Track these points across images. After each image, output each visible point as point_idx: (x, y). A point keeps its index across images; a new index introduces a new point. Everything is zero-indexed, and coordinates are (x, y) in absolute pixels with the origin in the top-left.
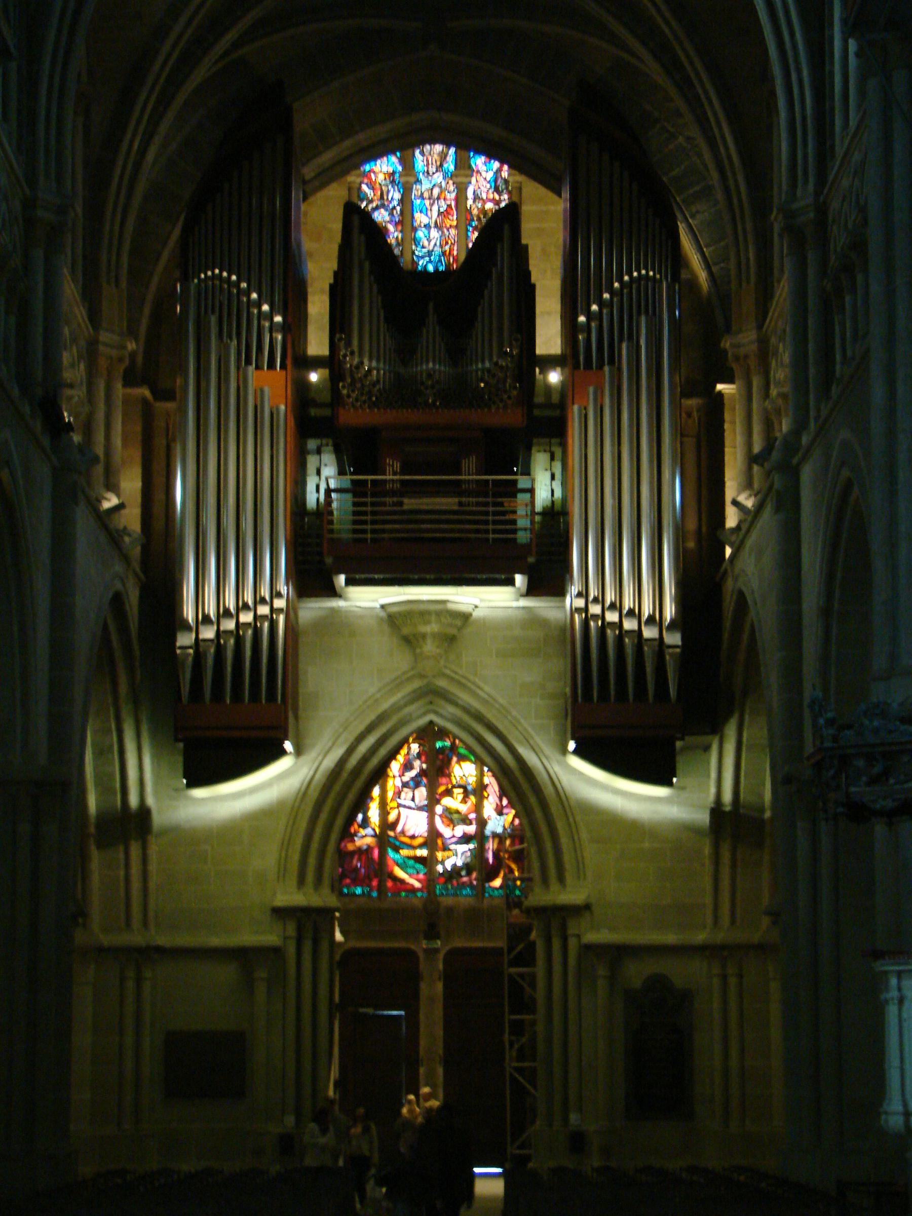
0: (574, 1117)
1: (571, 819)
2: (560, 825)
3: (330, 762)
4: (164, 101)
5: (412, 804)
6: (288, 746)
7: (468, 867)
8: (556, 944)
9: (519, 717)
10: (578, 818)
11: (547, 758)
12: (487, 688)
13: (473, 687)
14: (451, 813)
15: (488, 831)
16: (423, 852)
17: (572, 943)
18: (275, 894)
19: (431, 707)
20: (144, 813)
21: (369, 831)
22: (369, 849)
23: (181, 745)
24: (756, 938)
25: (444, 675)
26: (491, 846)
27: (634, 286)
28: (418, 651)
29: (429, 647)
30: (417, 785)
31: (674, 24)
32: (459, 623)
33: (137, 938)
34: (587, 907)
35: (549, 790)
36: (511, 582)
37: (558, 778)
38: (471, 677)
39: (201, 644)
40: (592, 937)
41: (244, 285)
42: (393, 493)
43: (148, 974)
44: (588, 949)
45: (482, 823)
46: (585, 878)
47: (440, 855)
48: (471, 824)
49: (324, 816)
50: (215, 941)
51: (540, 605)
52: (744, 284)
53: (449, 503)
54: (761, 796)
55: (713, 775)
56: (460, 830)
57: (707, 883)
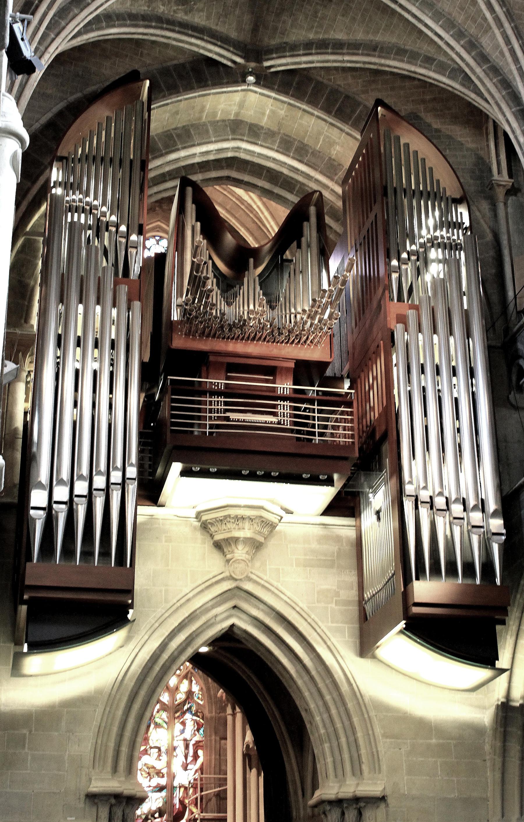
1: (366, 716)
3: (145, 655)
9: (316, 619)
10: (372, 714)
12: (288, 593)
13: (276, 591)
15: (176, 784)
18: (90, 780)
19: (234, 612)
25: (249, 579)
26: (178, 794)
28: (229, 556)
32: (266, 531)
34: (383, 799)
35: (344, 688)
36: (329, 482)
37: (353, 677)
38: (275, 584)
39: (55, 506)
45: (172, 777)
46: (380, 772)
49: (136, 706)
56: (157, 781)
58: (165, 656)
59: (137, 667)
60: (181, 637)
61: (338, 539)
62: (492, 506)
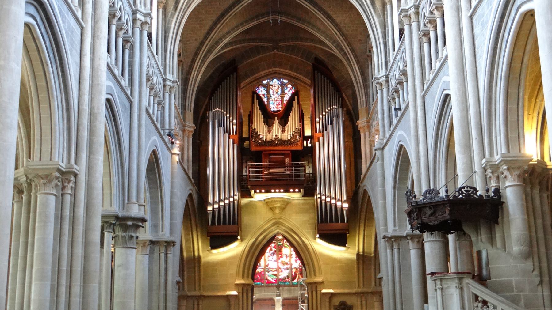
2: (315, 260)
4: (203, 62)
5: (272, 260)
6: (239, 237)
7: (288, 277)
8: (314, 293)
10: (319, 257)
11: (310, 240)
12: (293, 222)
14: (283, 262)
15: (293, 267)
16: (276, 273)
17: (319, 292)
19: (278, 228)
20: (199, 257)
21: (261, 267)
22: (261, 272)
23: (209, 237)
24: (370, 290)
26: (294, 270)
27: (332, 110)
29: (277, 211)
30: (274, 254)
31: (341, 38)
33: (197, 293)
34: (322, 282)
35: (311, 250)
38: (289, 219)
40: (324, 291)
41: (225, 113)
42: (267, 167)
43: (201, 303)
45: (291, 265)
46: (322, 274)
47: (280, 273)
48: (288, 265)
49: (249, 258)
52: (362, 107)
53: (282, 170)
54: (371, 249)
55: (357, 244)
56: (286, 266)
57: (356, 274)
58: (257, 243)
59: (248, 248)
60: (261, 237)
62: (345, 198)
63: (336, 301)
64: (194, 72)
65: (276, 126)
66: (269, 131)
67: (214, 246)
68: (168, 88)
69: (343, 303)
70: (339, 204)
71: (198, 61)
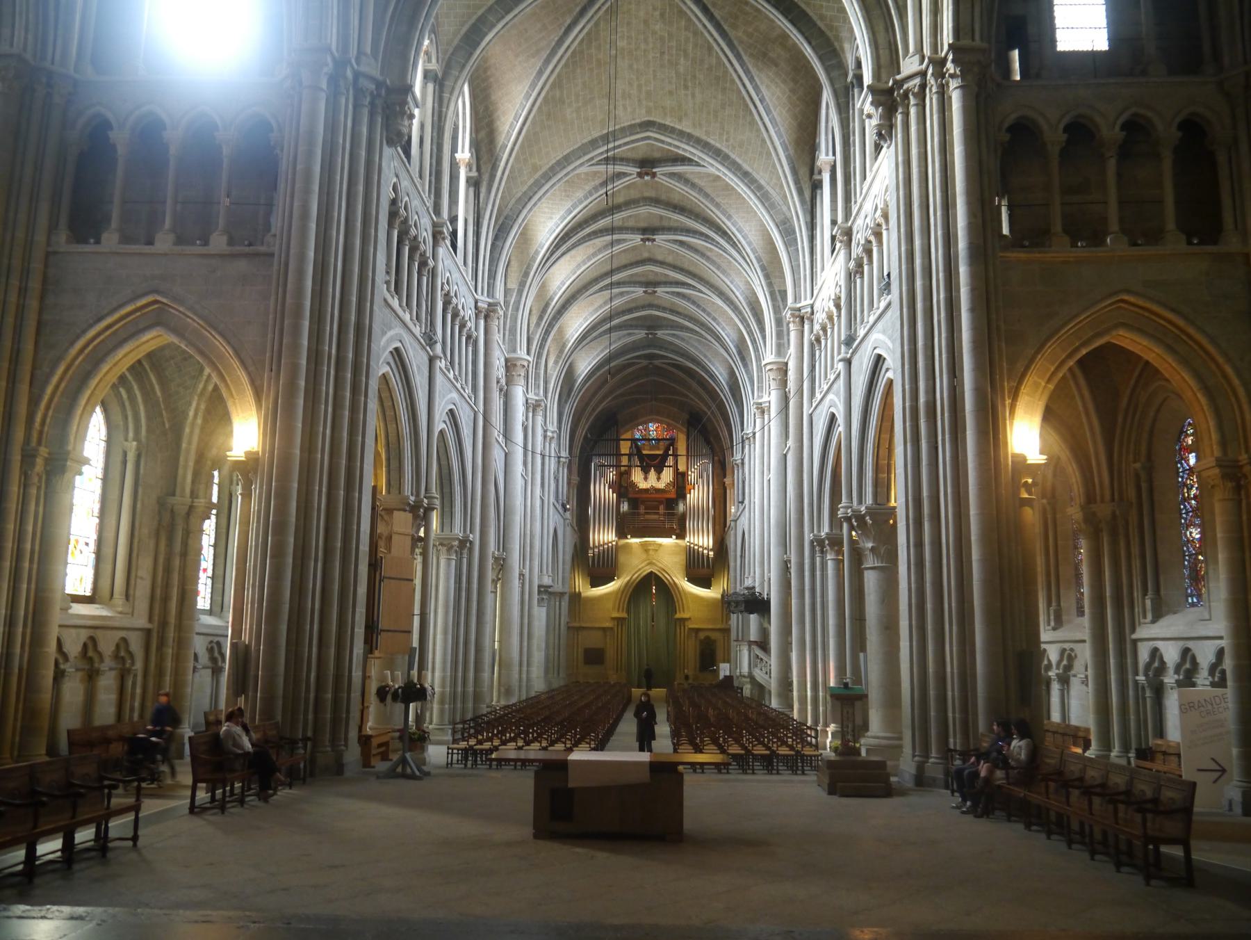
0: (686, 671)
4: (588, 420)
20: (580, 593)
29: (651, 552)
34: (690, 619)
40: (691, 626)
44: (690, 629)
50: (597, 625)
51: (678, 541)
60: (636, 575)
61: (680, 546)
62: (711, 546)
63: (702, 635)
64: (579, 431)
65: (652, 474)
66: (646, 479)
67: (594, 585)
68: (561, 464)
69: (708, 638)
70: (705, 552)
71: (583, 420)
